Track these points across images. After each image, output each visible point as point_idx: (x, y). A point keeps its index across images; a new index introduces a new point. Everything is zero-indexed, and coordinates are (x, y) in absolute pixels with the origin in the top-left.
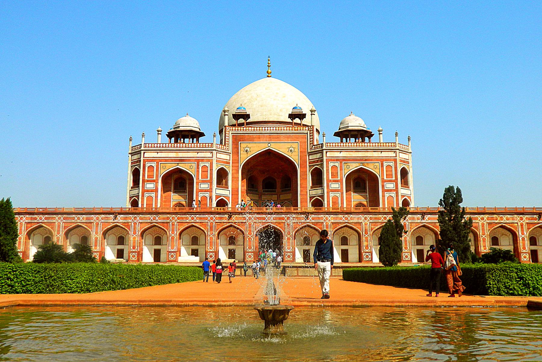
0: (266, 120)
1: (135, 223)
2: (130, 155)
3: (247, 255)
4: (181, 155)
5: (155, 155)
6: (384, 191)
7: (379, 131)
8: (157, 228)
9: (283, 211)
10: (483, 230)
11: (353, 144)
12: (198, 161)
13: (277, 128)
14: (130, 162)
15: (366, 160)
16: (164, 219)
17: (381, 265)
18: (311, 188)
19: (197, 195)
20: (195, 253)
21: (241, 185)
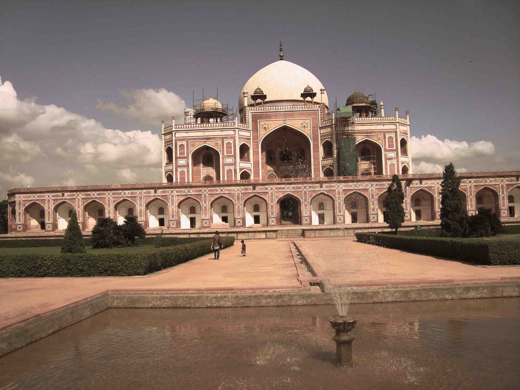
1: (173, 196)
2: (163, 136)
3: (270, 220)
4: (207, 134)
5: (184, 134)
6: (386, 159)
7: (381, 106)
9: (300, 181)
10: (471, 192)
12: (223, 138)
15: (371, 133)
16: (197, 191)
17: (387, 225)
18: (323, 158)
19: (223, 169)
20: (225, 219)
21: (261, 157)
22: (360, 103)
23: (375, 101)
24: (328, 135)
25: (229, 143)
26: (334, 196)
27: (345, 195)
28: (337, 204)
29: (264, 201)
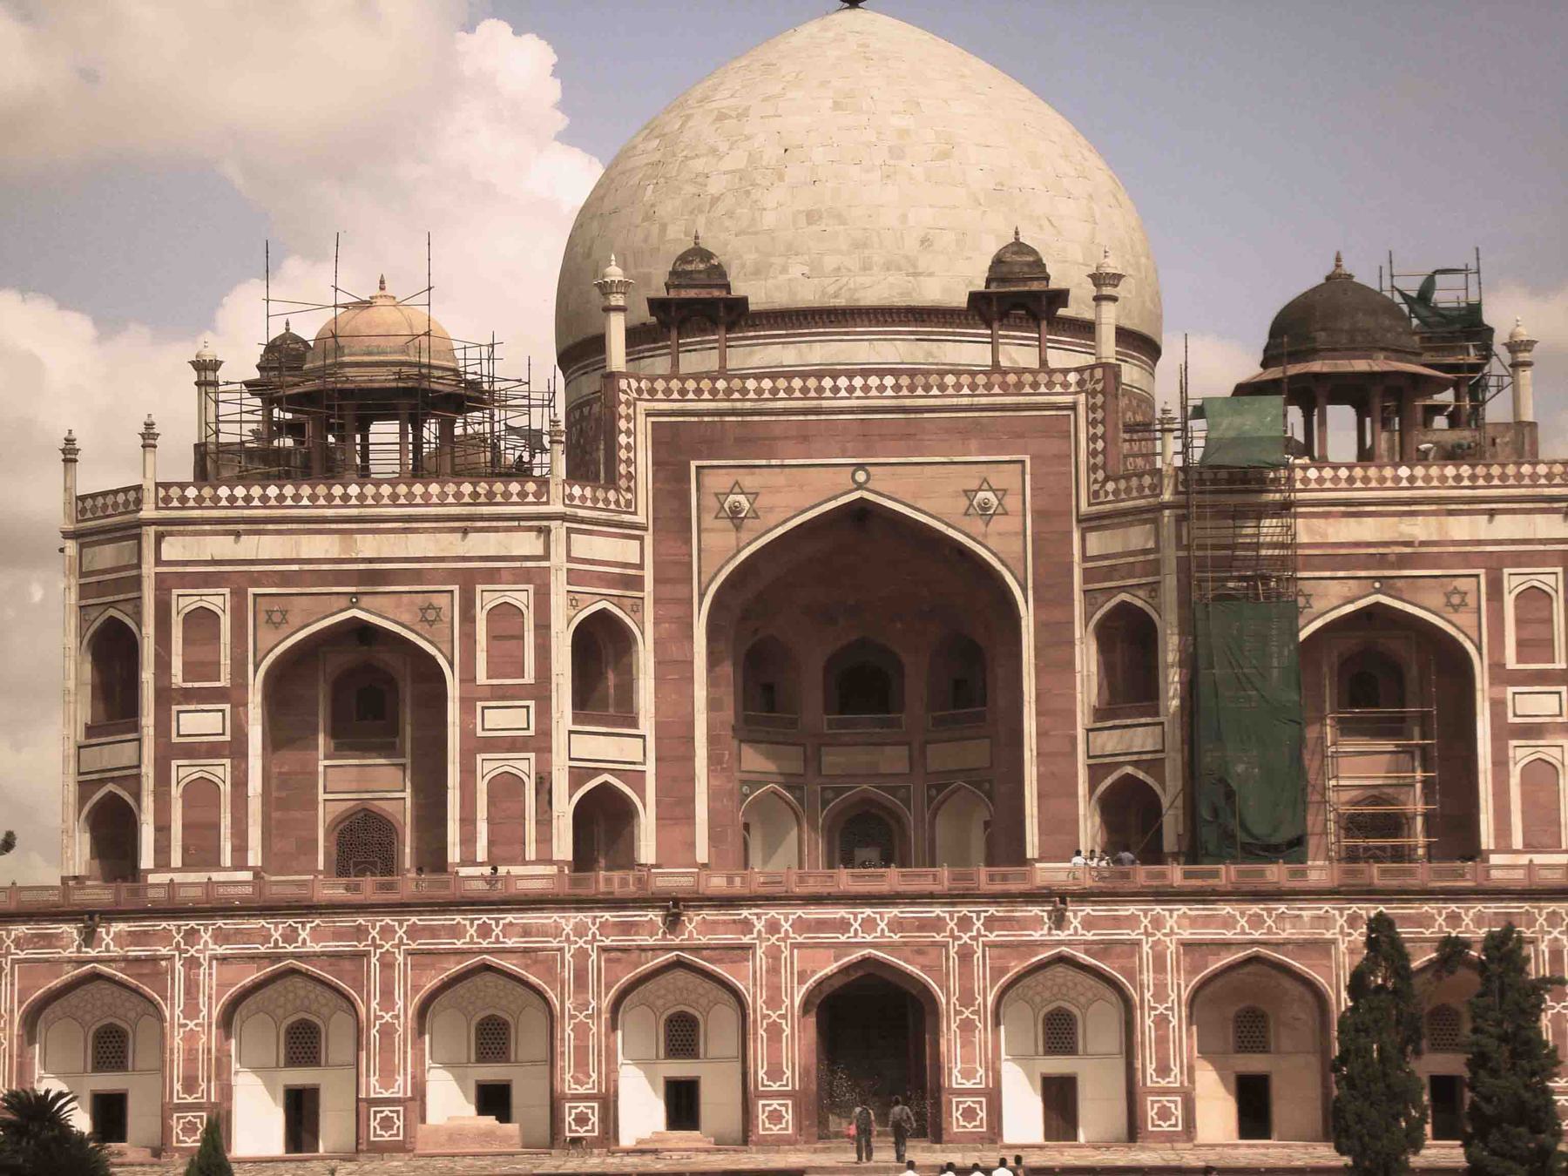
0: (841, 302)
1: (192, 963)
2: (71, 547)
3: (762, 1108)
4: (368, 546)
5: (220, 547)
6: (1504, 732)
7: (1514, 347)
8: (298, 981)
9: (936, 888)
11: (1328, 473)
12: (469, 579)
13: (905, 381)
14: (74, 581)
15: (1403, 561)
16: (339, 935)
19: (468, 772)
20: (494, 1100)
22: (1353, 351)
23: (1480, 304)
24: (1130, 570)
25: (505, 614)
26: (1131, 976)
27: (1193, 971)
28: (1146, 1023)
29: (726, 996)
